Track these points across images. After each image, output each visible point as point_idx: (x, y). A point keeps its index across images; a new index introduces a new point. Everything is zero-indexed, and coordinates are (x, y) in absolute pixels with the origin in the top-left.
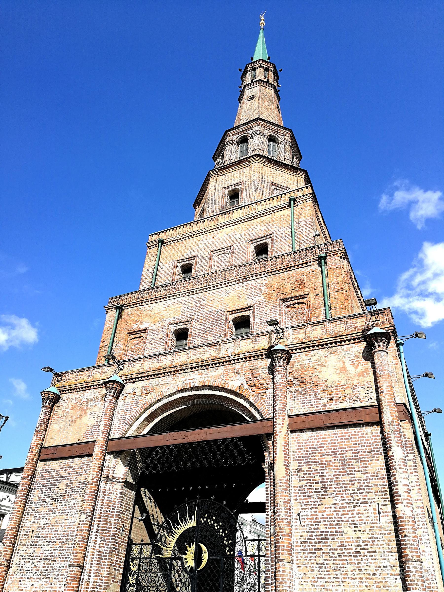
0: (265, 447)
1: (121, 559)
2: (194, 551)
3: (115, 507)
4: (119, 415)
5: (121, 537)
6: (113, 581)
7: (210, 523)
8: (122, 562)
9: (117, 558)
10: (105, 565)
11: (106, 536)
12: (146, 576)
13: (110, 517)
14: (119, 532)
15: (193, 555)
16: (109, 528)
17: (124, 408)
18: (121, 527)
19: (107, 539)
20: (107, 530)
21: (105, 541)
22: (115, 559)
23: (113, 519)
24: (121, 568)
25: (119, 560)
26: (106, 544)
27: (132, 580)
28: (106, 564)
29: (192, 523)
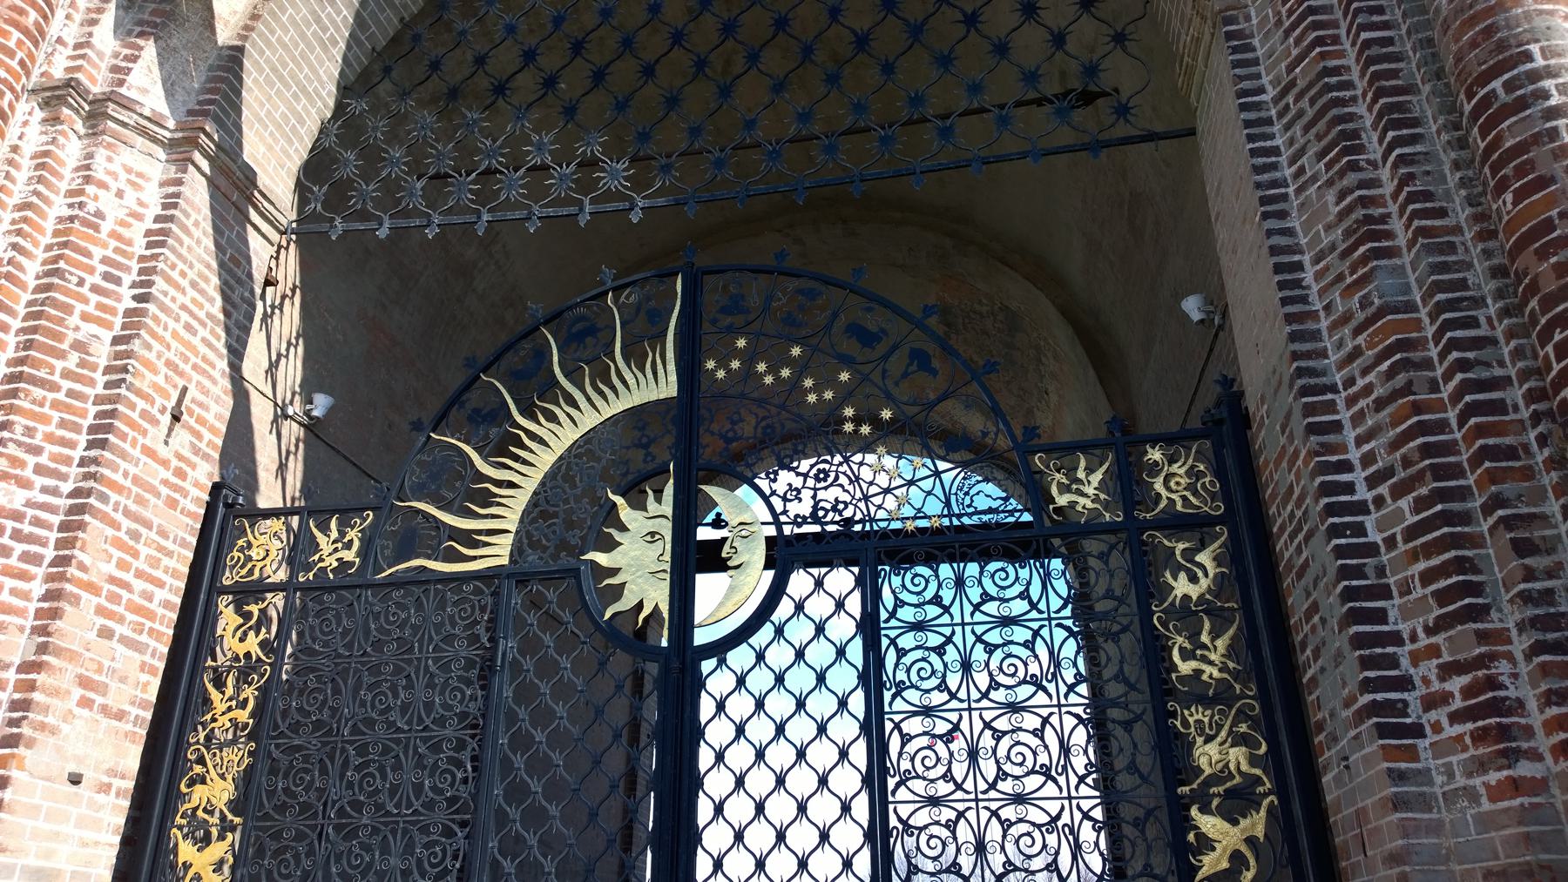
1: (160, 584)
2: (666, 529)
5: (163, 451)
6: (85, 703)
10: (26, 596)
11: (45, 419)
13: (86, 317)
14: (155, 422)
16: (67, 374)
19: (50, 438)
20: (54, 387)
21: (36, 451)
22: (111, 569)
23: (107, 336)
25: (139, 585)
26: (39, 470)
28: (37, 588)
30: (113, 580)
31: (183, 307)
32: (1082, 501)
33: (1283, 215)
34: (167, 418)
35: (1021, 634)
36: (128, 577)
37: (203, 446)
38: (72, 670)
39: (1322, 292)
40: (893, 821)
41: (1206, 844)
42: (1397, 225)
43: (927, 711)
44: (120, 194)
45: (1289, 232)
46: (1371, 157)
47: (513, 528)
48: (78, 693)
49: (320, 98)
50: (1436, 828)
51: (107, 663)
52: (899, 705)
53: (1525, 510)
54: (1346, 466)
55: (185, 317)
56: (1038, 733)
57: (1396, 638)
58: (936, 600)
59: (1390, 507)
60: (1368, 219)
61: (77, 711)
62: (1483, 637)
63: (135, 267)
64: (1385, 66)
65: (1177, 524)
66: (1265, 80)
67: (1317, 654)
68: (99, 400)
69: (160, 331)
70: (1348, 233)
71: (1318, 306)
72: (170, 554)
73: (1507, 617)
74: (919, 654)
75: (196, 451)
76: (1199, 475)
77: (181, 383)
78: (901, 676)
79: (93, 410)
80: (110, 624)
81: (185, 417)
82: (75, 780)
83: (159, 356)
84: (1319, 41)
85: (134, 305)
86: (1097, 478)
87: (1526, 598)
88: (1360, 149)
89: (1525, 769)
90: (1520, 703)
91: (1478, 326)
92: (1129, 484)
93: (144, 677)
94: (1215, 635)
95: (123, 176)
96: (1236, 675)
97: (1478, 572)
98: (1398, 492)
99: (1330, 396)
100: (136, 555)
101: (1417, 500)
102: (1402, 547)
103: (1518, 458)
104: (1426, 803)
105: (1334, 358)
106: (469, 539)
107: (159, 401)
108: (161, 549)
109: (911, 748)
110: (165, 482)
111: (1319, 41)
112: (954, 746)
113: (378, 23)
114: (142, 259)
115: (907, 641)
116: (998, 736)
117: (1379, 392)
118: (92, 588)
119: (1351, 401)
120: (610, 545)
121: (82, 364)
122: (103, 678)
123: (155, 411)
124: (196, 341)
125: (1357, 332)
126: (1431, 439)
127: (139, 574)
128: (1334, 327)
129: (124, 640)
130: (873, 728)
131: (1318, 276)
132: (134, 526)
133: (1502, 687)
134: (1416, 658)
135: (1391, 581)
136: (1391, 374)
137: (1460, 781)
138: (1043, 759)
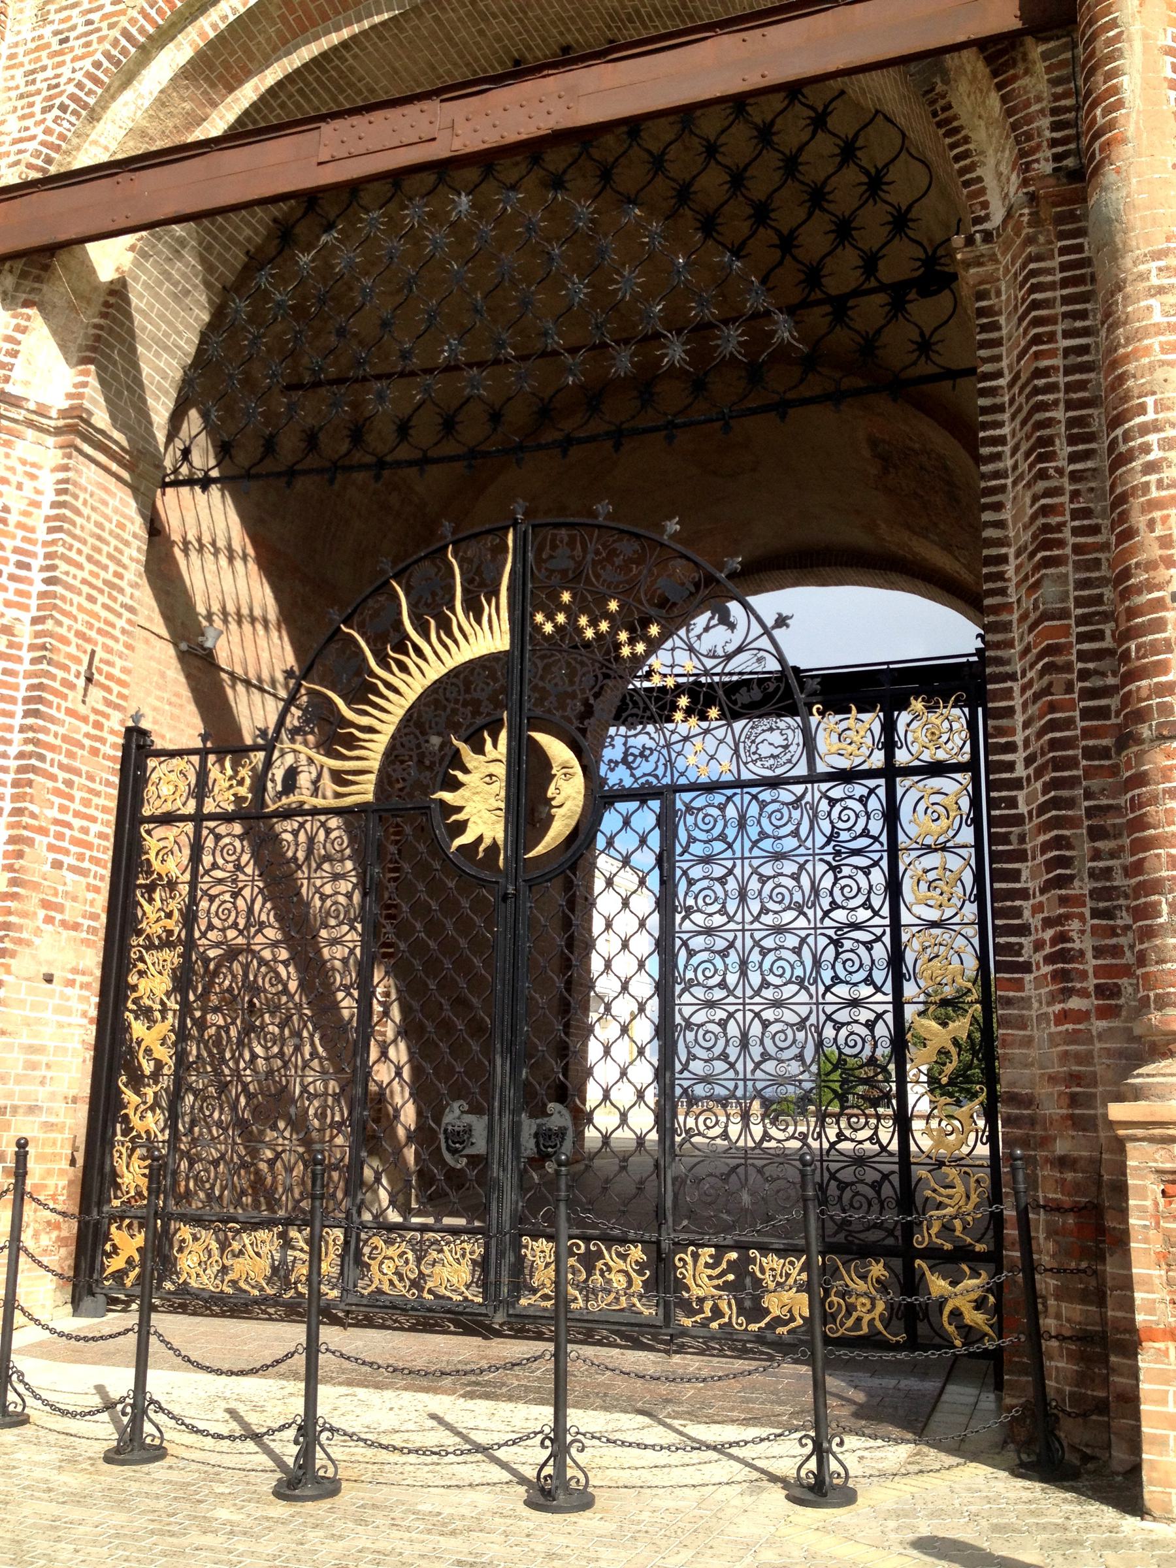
0: (966, 155)
1: (93, 819)
3: (33, 555)
4: (19, 73)
5: (82, 710)
6: (49, 920)
7: (589, 633)
8: (101, 836)
9: (63, 809)
12: (235, 895)
14: (72, 687)
15: (499, 787)
17: (47, 31)
18: (78, 661)
22: (54, 813)
23: (26, 617)
24: (95, 860)
25: (77, 823)
27: (154, 916)
29: (487, 637)
30: (57, 822)
31: (84, 581)
34: (81, 682)
35: (790, 867)
36: (68, 818)
37: (113, 698)
38: (35, 897)
39: (1018, 585)
40: (678, 1019)
42: (1066, 534)
43: (709, 931)
44: (20, 487)
46: (1059, 464)
48: (42, 913)
49: (179, 347)
51: (60, 888)
52: (687, 925)
53: (1105, 802)
54: (1011, 748)
55: (86, 589)
56: (797, 951)
57: (1024, 894)
58: (722, 837)
60: (1046, 528)
61: (43, 926)
62: (1064, 901)
63: (41, 551)
64: (1078, 377)
66: (1004, 363)
68: (28, 675)
69: (67, 607)
70: (1035, 537)
72: (98, 794)
73: (1082, 887)
74: (705, 883)
75: (108, 703)
77: (89, 648)
78: (690, 902)
79: (24, 683)
80: (60, 857)
81: (96, 676)
82: (49, 979)
83: (70, 628)
84: (1037, 339)
85: (44, 588)
87: (1093, 874)
88: (1051, 456)
89: (1075, 1003)
90: (1082, 953)
91: (1103, 639)
93: (91, 896)
95: (20, 469)
97: (1070, 847)
98: (1039, 773)
99: (1009, 684)
100: (71, 798)
101: (1045, 784)
103: (1109, 758)
105: (1019, 648)
107: (74, 668)
108: (91, 791)
109: (695, 961)
110: (87, 735)
111: (1037, 339)
112: (728, 960)
113: (225, 262)
114: (45, 544)
115: (696, 872)
116: (764, 952)
117: (1036, 687)
118: (43, 831)
119: (1024, 689)
121: (11, 645)
122: (59, 900)
123: (72, 678)
124: (97, 608)
125: (1031, 629)
126: (1058, 735)
127: (77, 814)
129: (72, 869)
130: (665, 945)
131: (1018, 568)
132: (68, 776)
133: (1072, 940)
135: (1028, 846)
136: (1042, 674)
137: (1045, 1009)
138: (799, 972)
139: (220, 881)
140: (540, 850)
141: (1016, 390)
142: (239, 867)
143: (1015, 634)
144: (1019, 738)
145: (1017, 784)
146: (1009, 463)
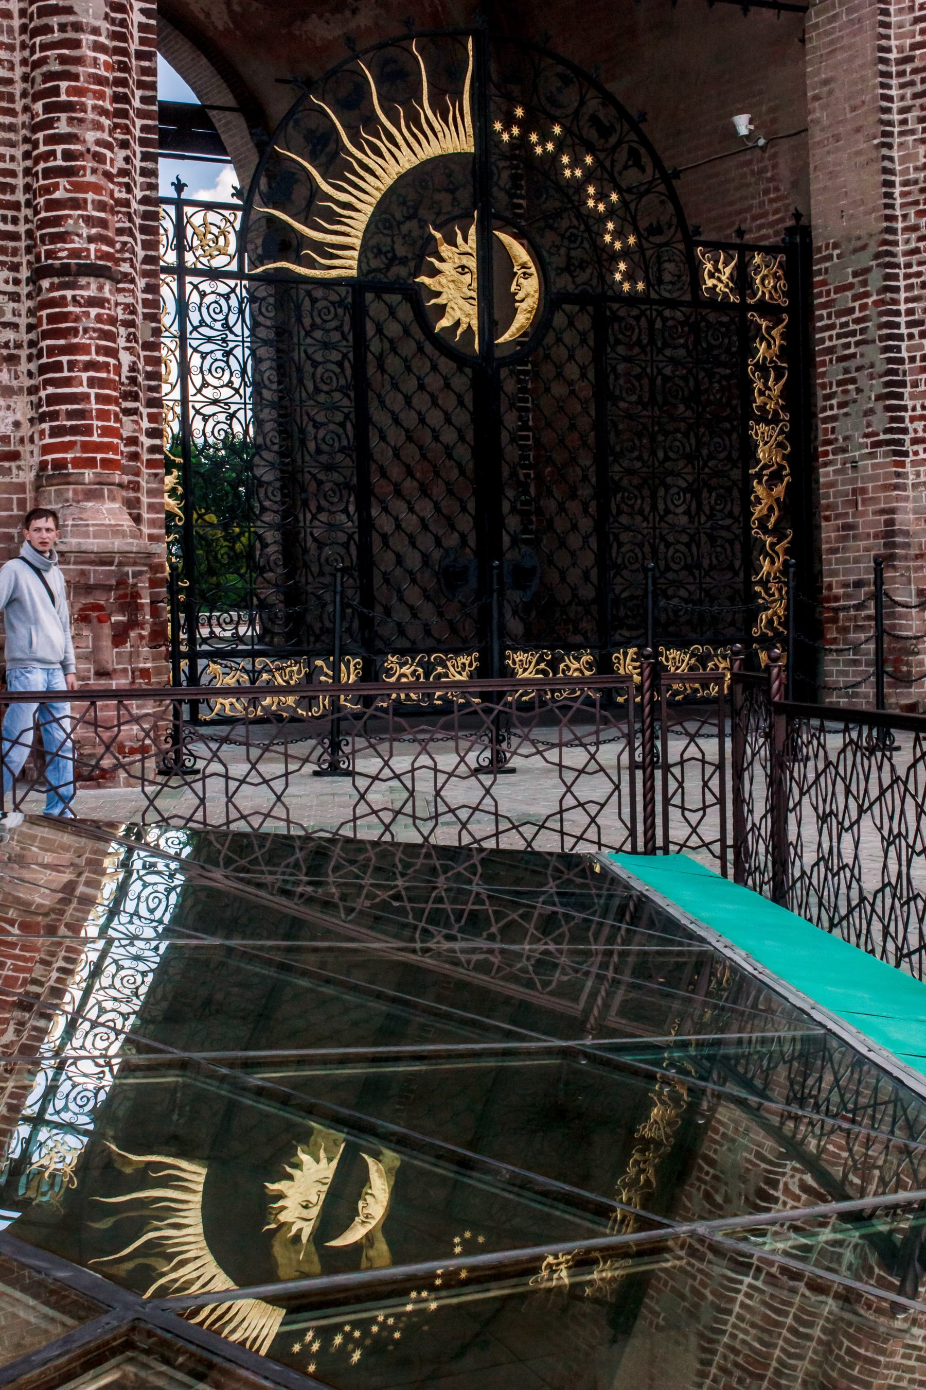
2: (472, 263)
12: (228, 354)
32: (720, 285)
33: (890, 146)
39: (903, 205)
41: (758, 501)
45: (891, 159)
47: (357, 242)
50: (906, 499)
54: (897, 313)
57: (904, 408)
59: (917, 341)
65: (764, 308)
67: (841, 405)
71: (898, 213)
76: (779, 278)
85: (144, 20)
86: (728, 270)
92: (742, 281)
94: (777, 380)
96: (782, 407)
102: (918, 364)
104: (903, 487)
105: (901, 248)
106: (319, 247)
119: (907, 276)
120: (434, 272)
128: (906, 229)
131: (903, 194)
134: (913, 419)
135: (908, 378)
139: (209, 339)
140: (506, 337)
141: (908, 68)
142: (227, 326)
143: (900, 238)
144: (903, 307)
145: (900, 337)
146: (896, 117)
